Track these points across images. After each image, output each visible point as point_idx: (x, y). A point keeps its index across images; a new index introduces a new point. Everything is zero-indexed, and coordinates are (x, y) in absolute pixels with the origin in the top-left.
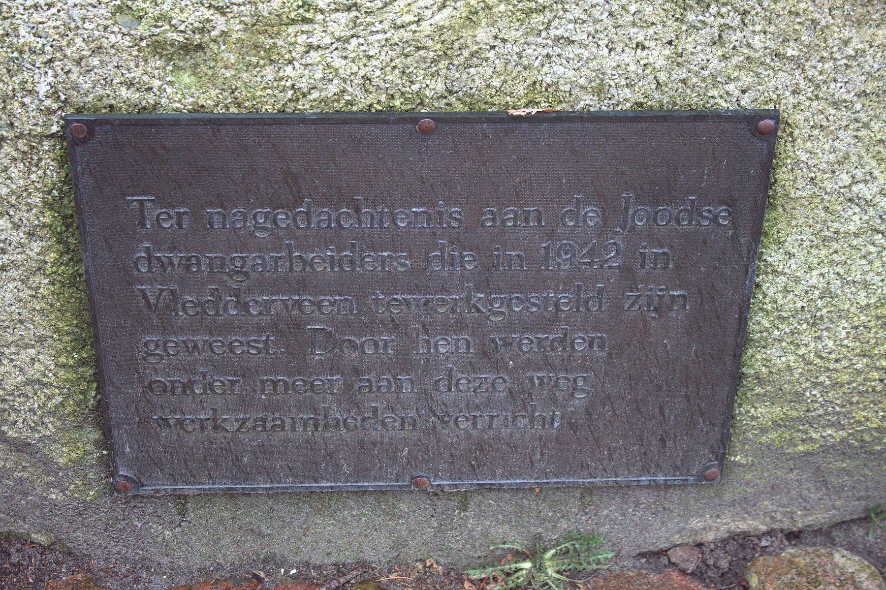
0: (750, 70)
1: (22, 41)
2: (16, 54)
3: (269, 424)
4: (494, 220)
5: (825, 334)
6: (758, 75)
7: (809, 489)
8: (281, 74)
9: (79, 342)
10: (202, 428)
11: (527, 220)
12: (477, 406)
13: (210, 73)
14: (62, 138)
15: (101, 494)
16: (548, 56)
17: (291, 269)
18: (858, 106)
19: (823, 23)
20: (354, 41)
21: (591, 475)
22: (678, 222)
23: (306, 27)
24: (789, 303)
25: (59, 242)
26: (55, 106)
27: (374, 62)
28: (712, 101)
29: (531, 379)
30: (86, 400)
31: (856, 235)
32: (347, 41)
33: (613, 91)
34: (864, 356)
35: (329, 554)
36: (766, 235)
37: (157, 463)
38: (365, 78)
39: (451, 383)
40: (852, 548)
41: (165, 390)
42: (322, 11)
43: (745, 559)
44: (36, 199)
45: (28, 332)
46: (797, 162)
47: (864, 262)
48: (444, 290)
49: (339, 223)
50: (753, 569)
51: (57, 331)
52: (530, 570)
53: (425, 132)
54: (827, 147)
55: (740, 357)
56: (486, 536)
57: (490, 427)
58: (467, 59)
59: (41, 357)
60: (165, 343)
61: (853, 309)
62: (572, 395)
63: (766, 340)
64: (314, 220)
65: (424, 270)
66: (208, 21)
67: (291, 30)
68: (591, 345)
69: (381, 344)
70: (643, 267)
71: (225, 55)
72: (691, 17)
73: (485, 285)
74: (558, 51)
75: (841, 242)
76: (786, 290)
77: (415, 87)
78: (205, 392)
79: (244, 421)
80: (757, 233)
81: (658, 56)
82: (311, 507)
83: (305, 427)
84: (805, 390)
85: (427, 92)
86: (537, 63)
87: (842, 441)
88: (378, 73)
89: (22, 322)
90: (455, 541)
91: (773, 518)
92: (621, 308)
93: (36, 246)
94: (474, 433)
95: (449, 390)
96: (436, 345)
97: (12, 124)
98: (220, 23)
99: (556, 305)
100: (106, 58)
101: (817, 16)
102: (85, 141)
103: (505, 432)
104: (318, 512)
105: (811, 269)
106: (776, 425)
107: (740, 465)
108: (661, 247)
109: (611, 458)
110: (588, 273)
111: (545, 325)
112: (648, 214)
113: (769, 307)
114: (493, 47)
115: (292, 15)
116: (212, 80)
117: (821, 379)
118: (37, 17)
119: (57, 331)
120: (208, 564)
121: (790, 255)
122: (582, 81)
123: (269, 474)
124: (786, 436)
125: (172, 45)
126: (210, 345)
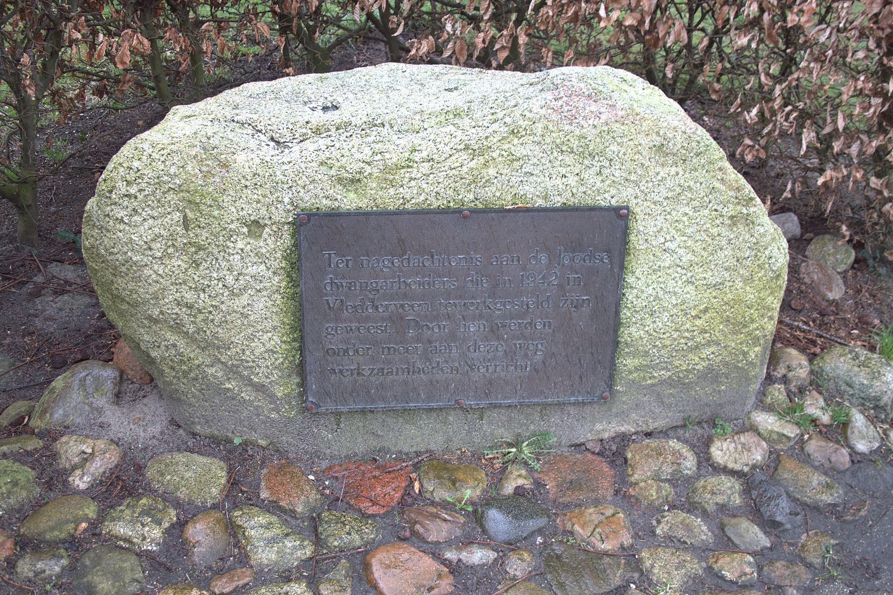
0: (614, 187)
1: (278, 178)
2: (275, 184)
3: (385, 371)
4: (497, 261)
5: (657, 319)
6: (618, 189)
7: (654, 406)
8: (397, 192)
9: (293, 329)
10: (352, 374)
11: (513, 261)
12: (489, 360)
13: (363, 192)
14: (294, 224)
15: (298, 413)
16: (522, 181)
17: (400, 288)
18: (665, 204)
19: (646, 165)
20: (432, 175)
21: (546, 398)
22: (584, 261)
23: (409, 170)
24: (640, 304)
25: (288, 277)
26: (292, 208)
27: (441, 185)
28: (598, 202)
29: (515, 345)
30: (295, 360)
31: (669, 268)
32: (428, 176)
33: (552, 198)
34: (677, 331)
35: (412, 446)
36: (626, 268)
37: (328, 394)
38: (437, 193)
39: (476, 348)
40: (678, 439)
41: (335, 353)
42: (416, 162)
43: (624, 446)
44: (279, 255)
45: (268, 325)
46: (639, 232)
47: (673, 282)
48: (473, 298)
49: (423, 263)
50: (629, 450)
51: (283, 323)
52: (515, 453)
53: (465, 217)
54: (652, 224)
55: (617, 332)
56: (493, 435)
57: (495, 371)
58: (484, 183)
59: (274, 337)
60: (336, 328)
61: (670, 306)
62: (536, 353)
63: (629, 323)
64: (412, 263)
65: (464, 287)
66: (363, 168)
67: (402, 171)
68: (544, 326)
69: (442, 327)
70: (569, 284)
71: (370, 184)
72: (586, 162)
73: (493, 295)
74: (526, 179)
75: (662, 271)
76: (637, 297)
77: (460, 197)
78: (354, 355)
79: (373, 369)
80: (622, 267)
81: (572, 180)
82: (404, 419)
83: (403, 372)
84: (649, 349)
85: (466, 199)
86: (517, 185)
87: (669, 377)
88: (443, 190)
89: (266, 319)
90: (477, 438)
91: (637, 424)
92: (558, 306)
93: (277, 279)
94: (487, 375)
95: (475, 351)
96: (469, 327)
97: (271, 218)
98: (368, 169)
99: (527, 305)
100: (317, 185)
101: (643, 161)
102: (306, 224)
103: (503, 374)
104: (407, 422)
105: (649, 286)
106: (636, 369)
107: (620, 392)
108: (577, 274)
109: (555, 388)
110: (542, 288)
111: (522, 316)
112: (570, 257)
113: (629, 306)
114: (496, 177)
115: (403, 164)
116: (365, 195)
117: (657, 343)
118: (285, 167)
119: (283, 323)
120: (350, 453)
121: (639, 279)
122: (538, 193)
123: (384, 399)
124: (642, 375)
125: (346, 179)
126: (359, 329)
